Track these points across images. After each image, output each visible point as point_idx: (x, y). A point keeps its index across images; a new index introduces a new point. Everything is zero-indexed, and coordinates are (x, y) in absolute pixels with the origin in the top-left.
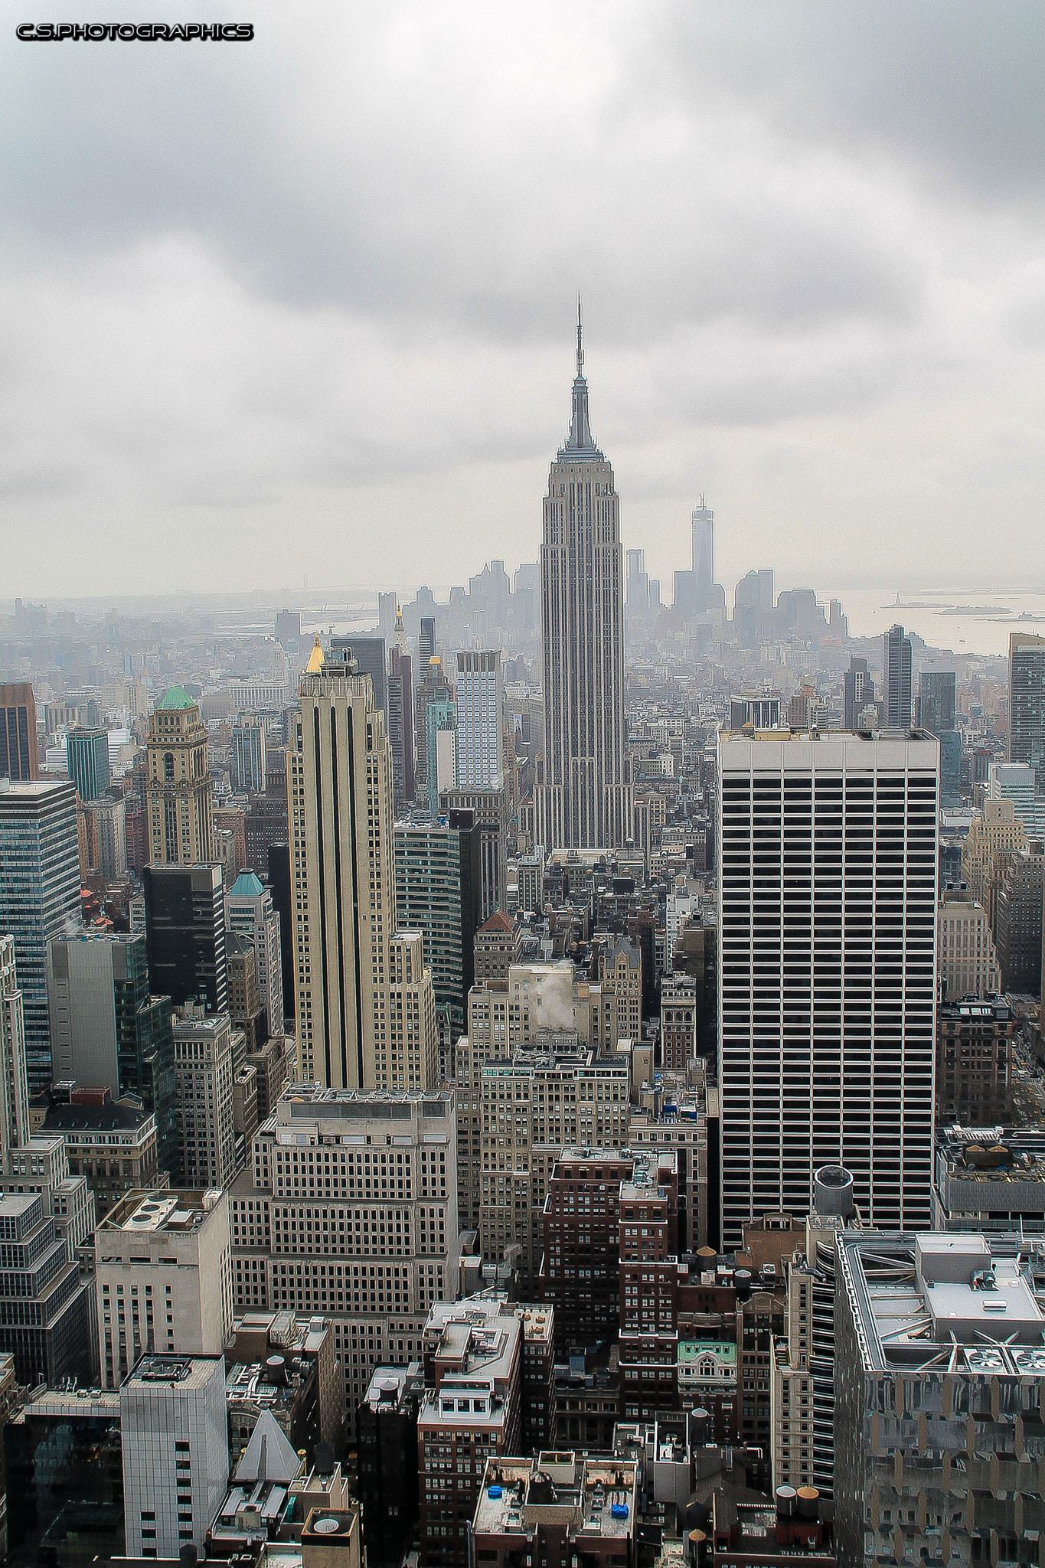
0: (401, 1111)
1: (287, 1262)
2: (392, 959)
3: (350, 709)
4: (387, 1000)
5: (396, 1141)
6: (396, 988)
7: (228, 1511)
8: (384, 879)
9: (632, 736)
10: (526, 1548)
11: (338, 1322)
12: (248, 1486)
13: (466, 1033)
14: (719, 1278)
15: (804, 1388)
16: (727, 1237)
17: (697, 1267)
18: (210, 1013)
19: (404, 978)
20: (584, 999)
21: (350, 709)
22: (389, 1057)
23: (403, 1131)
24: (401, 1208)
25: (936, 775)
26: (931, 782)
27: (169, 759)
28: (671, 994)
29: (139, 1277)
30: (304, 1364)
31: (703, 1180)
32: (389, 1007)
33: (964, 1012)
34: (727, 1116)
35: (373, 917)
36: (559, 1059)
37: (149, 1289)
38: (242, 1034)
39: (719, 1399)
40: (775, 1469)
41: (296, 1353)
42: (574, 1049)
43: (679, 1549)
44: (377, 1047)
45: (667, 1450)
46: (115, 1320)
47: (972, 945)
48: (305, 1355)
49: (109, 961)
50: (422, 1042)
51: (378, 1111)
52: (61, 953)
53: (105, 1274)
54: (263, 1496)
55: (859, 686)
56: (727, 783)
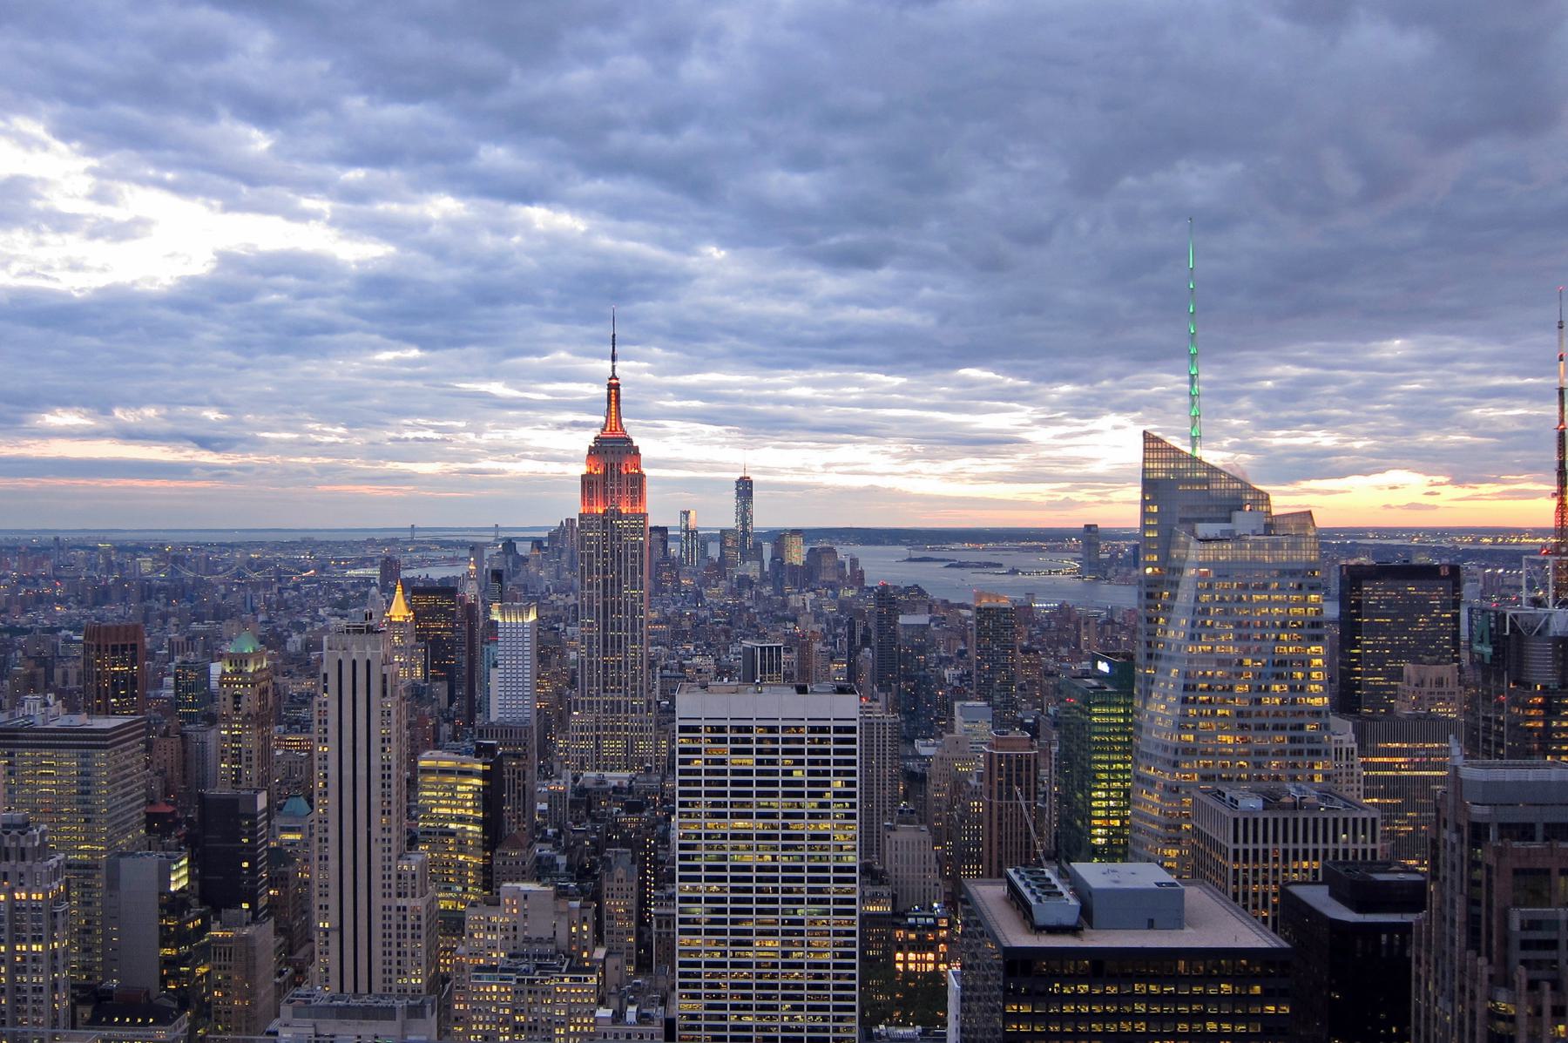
0: (389, 1014)
2: (399, 877)
4: (394, 912)
6: (401, 902)
8: (394, 808)
19: (409, 894)
20: (563, 913)
28: (662, 904)
32: (396, 919)
36: (539, 967)
44: (384, 954)
47: (919, 863)
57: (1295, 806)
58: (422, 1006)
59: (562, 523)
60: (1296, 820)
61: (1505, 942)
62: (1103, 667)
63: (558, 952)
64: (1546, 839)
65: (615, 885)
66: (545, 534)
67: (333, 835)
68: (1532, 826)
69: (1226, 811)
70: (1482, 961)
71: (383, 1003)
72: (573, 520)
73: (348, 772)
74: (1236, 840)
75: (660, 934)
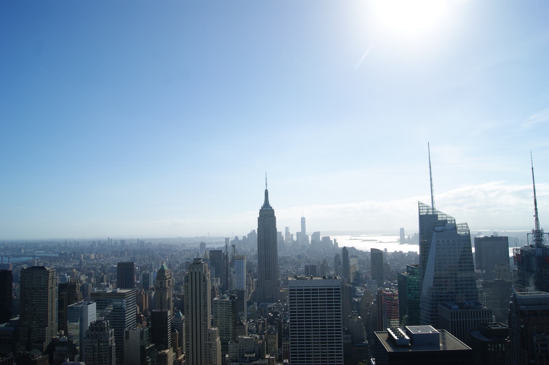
3: (200, 272)
4: (208, 345)
13: (227, 353)
21: (200, 272)
22: (208, 360)
26: (339, 289)
27: (161, 283)
28: (284, 342)
33: (357, 345)
35: (205, 324)
38: (175, 353)
42: (254, 357)
44: (205, 357)
49: (139, 335)
52: (127, 332)
59: (251, 231)
60: (468, 312)
66: (247, 235)
67: (190, 323)
72: (254, 231)
74: (452, 318)
75: (284, 350)
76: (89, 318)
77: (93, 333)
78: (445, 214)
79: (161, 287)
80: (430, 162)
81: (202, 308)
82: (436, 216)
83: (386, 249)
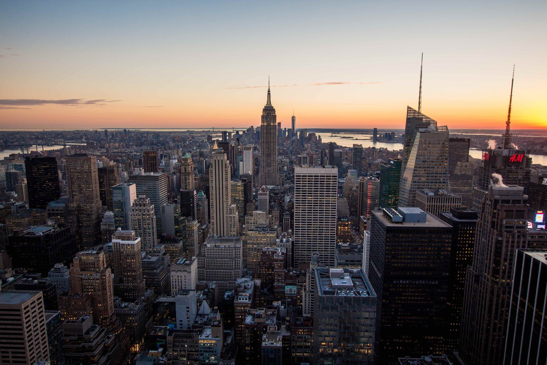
0: (232, 240)
1: (209, 270)
4: (229, 218)
5: (230, 246)
6: (231, 215)
7: (197, 320)
9: (278, 162)
10: (255, 326)
11: (219, 282)
12: (201, 315)
14: (293, 273)
15: (309, 295)
16: (295, 265)
17: (289, 271)
18: (194, 219)
23: (232, 245)
24: (232, 260)
25: (337, 175)
26: (336, 176)
29: (179, 274)
30: (212, 291)
31: (291, 254)
33: (342, 220)
34: (296, 241)
36: (263, 230)
37: (181, 277)
38: (199, 224)
39: (293, 297)
40: (303, 310)
41: (210, 289)
43: (284, 326)
45: (283, 307)
46: (174, 282)
48: (212, 289)
49: (173, 210)
50: (236, 226)
51: (227, 241)
52: (163, 207)
53: (172, 273)
54: (204, 317)
55: (324, 154)
56: (297, 176)
57: (443, 195)
58: (239, 239)
61: (501, 226)
62: (392, 162)
63: (267, 226)
64: (512, 203)
65: (274, 211)
67: (214, 200)
68: (509, 200)
69: (426, 196)
70: (495, 231)
71: (230, 238)
73: (218, 186)
76: (131, 196)
77: (137, 208)
78: (428, 118)
79: (185, 170)
80: (421, 72)
81: (224, 189)
82: (422, 118)
83: (361, 145)
